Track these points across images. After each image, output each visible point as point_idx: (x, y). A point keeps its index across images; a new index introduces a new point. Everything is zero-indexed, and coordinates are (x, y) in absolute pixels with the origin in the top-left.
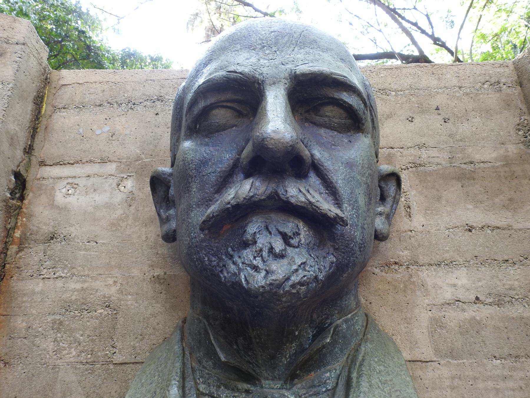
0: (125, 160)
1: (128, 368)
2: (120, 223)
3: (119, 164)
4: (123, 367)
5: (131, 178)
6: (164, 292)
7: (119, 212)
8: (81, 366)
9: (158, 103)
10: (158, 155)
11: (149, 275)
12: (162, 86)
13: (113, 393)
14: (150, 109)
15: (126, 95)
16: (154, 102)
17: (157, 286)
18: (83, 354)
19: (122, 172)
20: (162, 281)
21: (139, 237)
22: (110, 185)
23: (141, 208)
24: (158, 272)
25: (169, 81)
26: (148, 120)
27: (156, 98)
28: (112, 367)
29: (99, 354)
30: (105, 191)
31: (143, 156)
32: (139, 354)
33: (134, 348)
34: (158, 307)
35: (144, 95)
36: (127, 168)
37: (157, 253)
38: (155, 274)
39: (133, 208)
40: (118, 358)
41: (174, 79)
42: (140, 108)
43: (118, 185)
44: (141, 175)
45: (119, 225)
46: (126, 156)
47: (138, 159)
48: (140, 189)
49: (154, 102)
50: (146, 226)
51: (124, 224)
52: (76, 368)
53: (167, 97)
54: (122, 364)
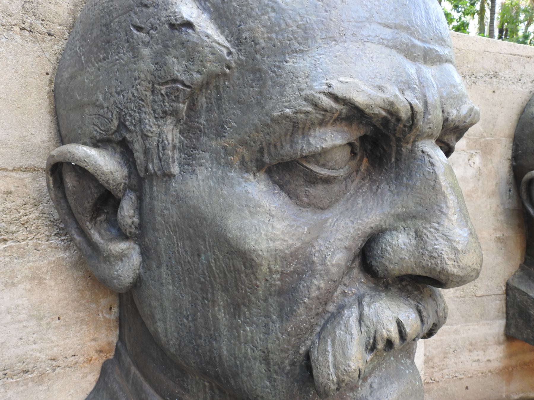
0: (472, 137)
1: (484, 298)
2: (473, 194)
3: (468, 141)
4: (481, 298)
5: (478, 155)
6: (503, 249)
7: (471, 185)
8: (457, 299)
9: (494, 80)
10: (496, 135)
11: (493, 237)
12: (497, 61)
13: (477, 314)
14: (489, 85)
15: (469, 66)
16: (491, 78)
17: (499, 244)
18: (458, 292)
19: (471, 148)
20: (502, 241)
21: (486, 206)
22: (464, 160)
23: (486, 183)
24: (499, 234)
25: (501, 55)
26: (488, 97)
27: (492, 73)
28: (475, 298)
29: (468, 291)
30: (460, 165)
31: (485, 134)
32: (491, 290)
33: (488, 286)
34: (500, 259)
35: (483, 68)
36: (474, 145)
37: (498, 220)
38: (498, 236)
39: (481, 182)
40: (479, 293)
41: (505, 53)
42: (480, 82)
43: (469, 160)
44: (485, 153)
45: (472, 196)
46: (473, 133)
47: (482, 137)
48: (484, 166)
49: (491, 78)
50: (490, 197)
51: (475, 196)
52: (454, 301)
53: (500, 74)
54: (481, 296)
